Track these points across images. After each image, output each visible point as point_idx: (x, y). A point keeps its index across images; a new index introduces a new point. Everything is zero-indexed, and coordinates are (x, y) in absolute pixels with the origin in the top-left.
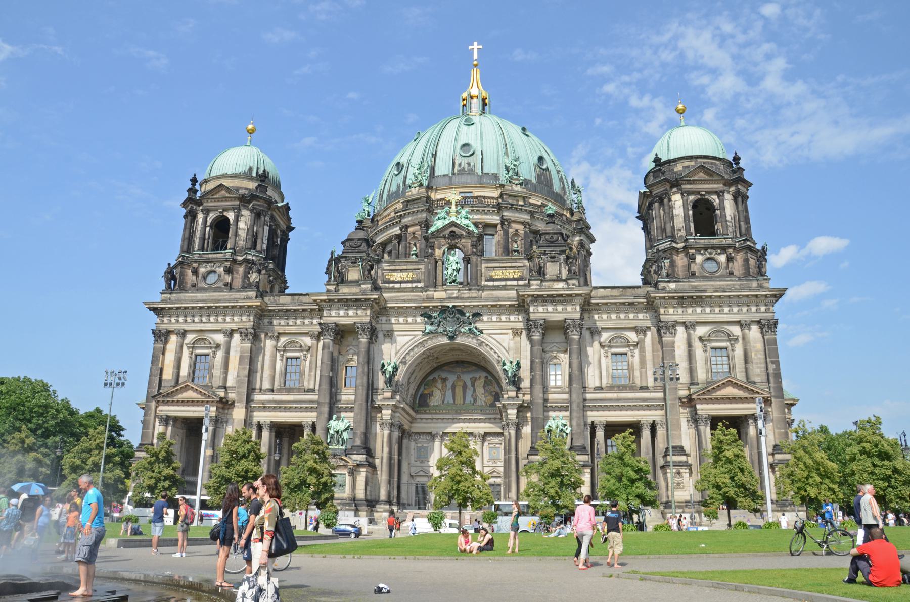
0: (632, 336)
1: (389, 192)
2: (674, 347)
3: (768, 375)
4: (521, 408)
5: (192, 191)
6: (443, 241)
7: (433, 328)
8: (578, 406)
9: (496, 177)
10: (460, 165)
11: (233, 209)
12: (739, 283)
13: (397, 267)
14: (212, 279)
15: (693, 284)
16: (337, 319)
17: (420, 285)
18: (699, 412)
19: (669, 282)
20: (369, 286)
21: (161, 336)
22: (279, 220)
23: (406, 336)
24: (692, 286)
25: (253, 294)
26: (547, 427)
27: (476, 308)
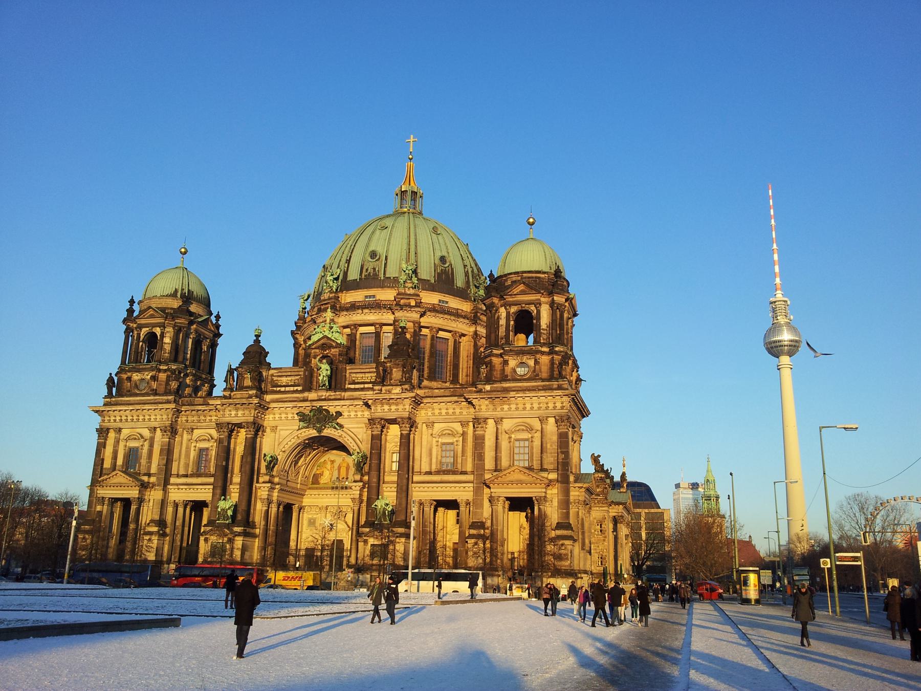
0: (458, 427)
2: (484, 440)
4: (361, 490)
5: (130, 311)
6: (317, 351)
7: (305, 425)
8: (401, 489)
9: (396, 280)
10: (367, 270)
13: (284, 374)
15: (504, 386)
17: (300, 388)
18: (493, 495)
22: (203, 331)
23: (287, 430)
24: (503, 387)
25: (171, 398)
26: (373, 506)
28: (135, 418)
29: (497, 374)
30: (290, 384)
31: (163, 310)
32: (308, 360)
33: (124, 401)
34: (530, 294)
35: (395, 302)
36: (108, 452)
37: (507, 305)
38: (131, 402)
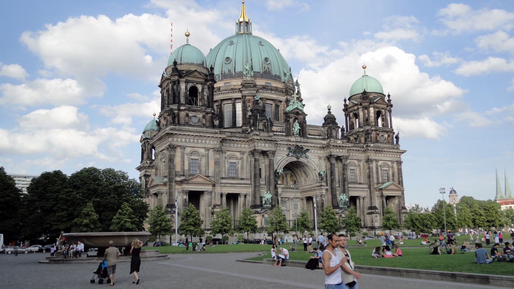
1: (222, 72)
2: (373, 169)
3: (399, 181)
4: (327, 190)
6: (293, 115)
10: (265, 68)
11: (202, 84)
12: (392, 146)
14: (195, 120)
15: (378, 145)
16: (262, 148)
18: (384, 194)
19: (371, 143)
20: (273, 134)
21: (172, 148)
24: (378, 146)
27: (308, 147)
28: (196, 141)
29: (373, 140)
30: (278, 131)
31: (200, 73)
32: (288, 119)
33: (185, 129)
34: (383, 104)
35: (284, 90)
36: (178, 160)
37: (374, 107)
38: (190, 130)
